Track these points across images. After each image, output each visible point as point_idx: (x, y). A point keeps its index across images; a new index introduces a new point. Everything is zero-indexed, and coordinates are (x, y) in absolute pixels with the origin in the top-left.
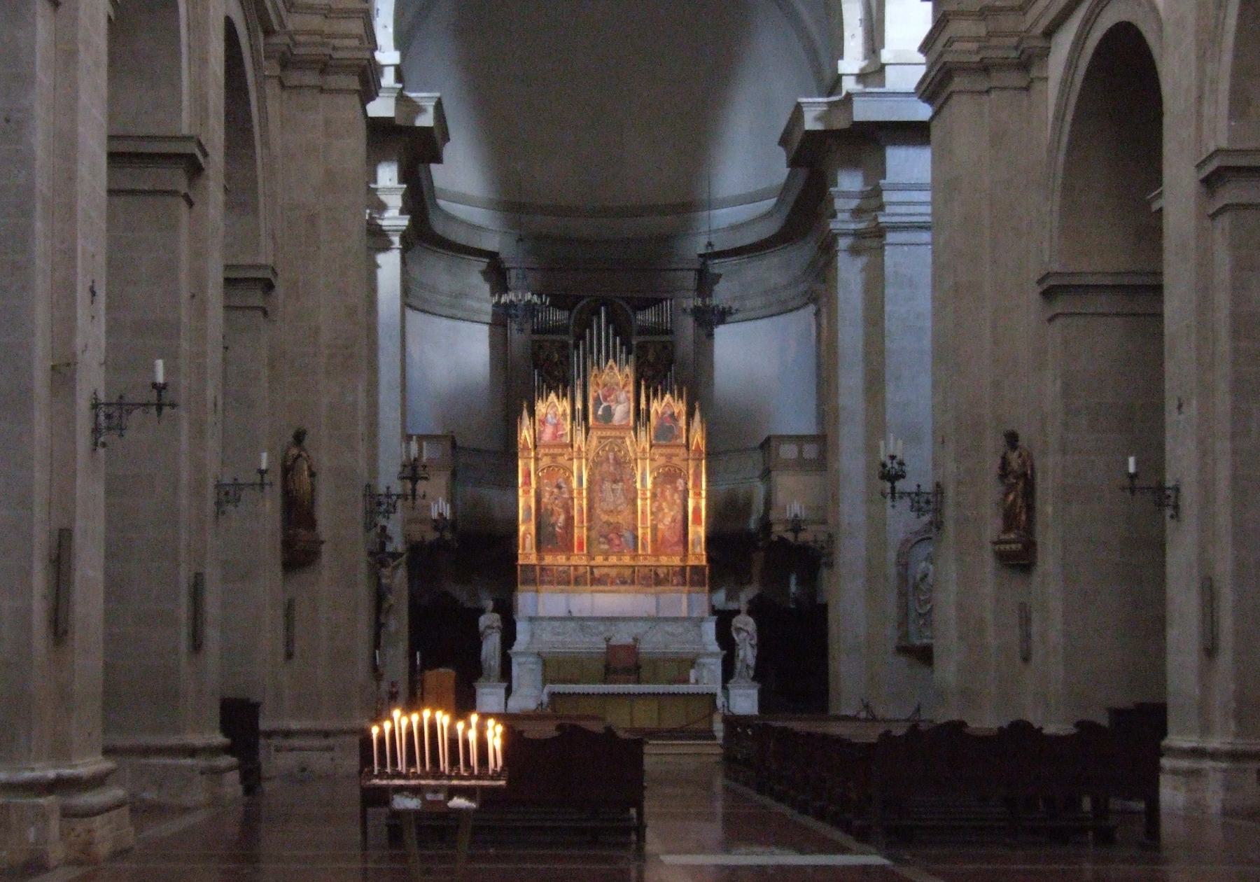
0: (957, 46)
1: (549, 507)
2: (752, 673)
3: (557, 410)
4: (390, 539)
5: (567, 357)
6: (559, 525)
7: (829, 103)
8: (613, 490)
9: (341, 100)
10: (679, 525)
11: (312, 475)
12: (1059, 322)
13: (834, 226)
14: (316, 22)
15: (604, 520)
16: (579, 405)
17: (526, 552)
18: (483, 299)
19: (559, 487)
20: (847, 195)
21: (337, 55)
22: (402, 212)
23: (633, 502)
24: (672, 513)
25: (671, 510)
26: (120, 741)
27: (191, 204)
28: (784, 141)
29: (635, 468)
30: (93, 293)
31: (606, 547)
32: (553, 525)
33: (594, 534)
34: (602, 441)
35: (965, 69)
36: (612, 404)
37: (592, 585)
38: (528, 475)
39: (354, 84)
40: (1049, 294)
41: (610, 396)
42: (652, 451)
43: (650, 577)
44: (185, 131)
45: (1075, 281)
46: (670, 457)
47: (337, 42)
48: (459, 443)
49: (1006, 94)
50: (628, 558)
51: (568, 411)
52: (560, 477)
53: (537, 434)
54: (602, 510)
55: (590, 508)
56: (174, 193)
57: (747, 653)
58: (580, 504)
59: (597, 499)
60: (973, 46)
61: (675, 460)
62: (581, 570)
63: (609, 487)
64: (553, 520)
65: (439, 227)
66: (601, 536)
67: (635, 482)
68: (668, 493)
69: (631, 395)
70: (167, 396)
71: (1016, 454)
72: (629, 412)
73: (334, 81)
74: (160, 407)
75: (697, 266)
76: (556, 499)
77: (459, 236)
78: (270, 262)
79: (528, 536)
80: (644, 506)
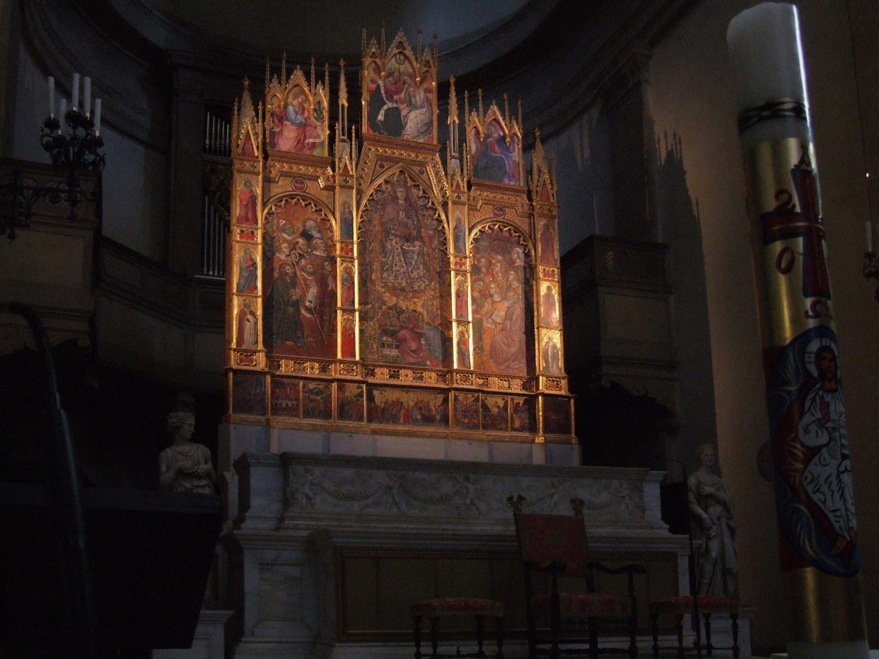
1: (288, 270)
3: (307, 99)
6: (307, 304)
8: (404, 253)
15: (389, 305)
16: (343, 101)
17: (244, 347)
19: (307, 236)
23: (443, 276)
24: (507, 304)
25: (504, 298)
29: (443, 217)
31: (394, 352)
32: (296, 305)
34: (385, 164)
36: (401, 106)
37: (370, 421)
41: (397, 93)
42: (472, 193)
43: (476, 411)
46: (500, 209)
50: (434, 375)
52: (309, 219)
53: (267, 136)
54: (385, 285)
59: (376, 266)
61: (510, 215)
62: (352, 390)
63: (398, 246)
64: (296, 294)
66: (385, 332)
67: (444, 243)
69: (433, 97)
72: (431, 122)
76: (301, 256)
79: (249, 317)
80: (461, 284)
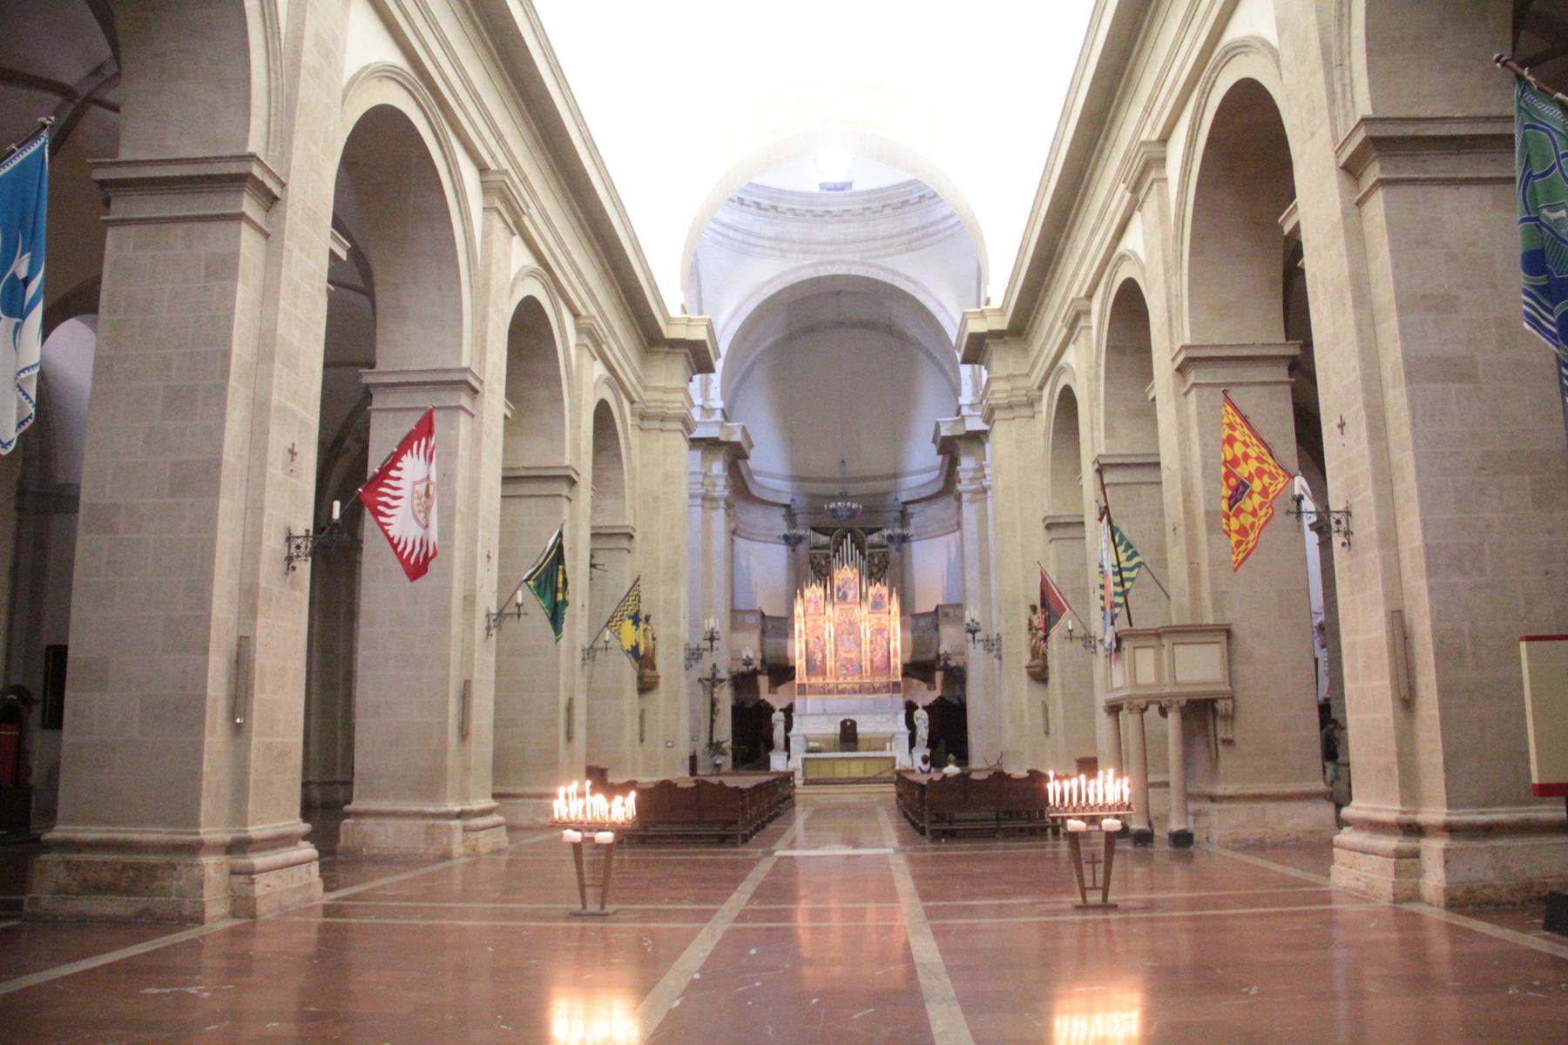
0: (996, 395)
2: (926, 743)
4: (718, 671)
5: (829, 562)
7: (954, 421)
9: (673, 435)
10: (885, 659)
11: (654, 639)
12: (1054, 542)
13: (959, 487)
14: (658, 395)
16: (828, 591)
18: (782, 528)
19: (818, 638)
20: (965, 470)
21: (669, 412)
22: (725, 488)
23: (860, 645)
26: (501, 790)
27: (570, 500)
28: (934, 441)
30: (489, 557)
31: (845, 672)
33: (838, 665)
35: (999, 407)
38: (800, 632)
39: (679, 426)
40: (1049, 527)
44: (567, 463)
45: (1062, 520)
46: (879, 619)
47: (670, 405)
48: (767, 613)
49: (1024, 420)
51: (823, 595)
55: (836, 650)
56: (560, 496)
57: (923, 732)
58: (830, 648)
60: (1004, 395)
61: (883, 621)
62: (831, 686)
65: (756, 492)
68: (879, 639)
70: (522, 611)
71: (1036, 617)
73: (669, 425)
74: (519, 615)
75: (901, 509)
77: (769, 497)
78: (632, 524)
